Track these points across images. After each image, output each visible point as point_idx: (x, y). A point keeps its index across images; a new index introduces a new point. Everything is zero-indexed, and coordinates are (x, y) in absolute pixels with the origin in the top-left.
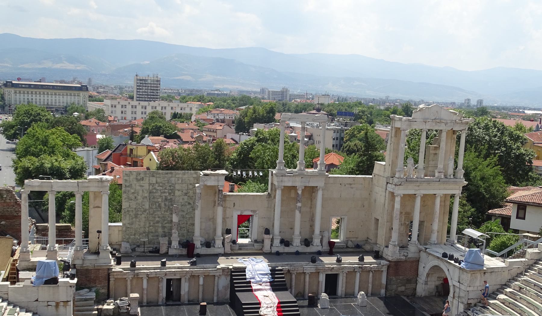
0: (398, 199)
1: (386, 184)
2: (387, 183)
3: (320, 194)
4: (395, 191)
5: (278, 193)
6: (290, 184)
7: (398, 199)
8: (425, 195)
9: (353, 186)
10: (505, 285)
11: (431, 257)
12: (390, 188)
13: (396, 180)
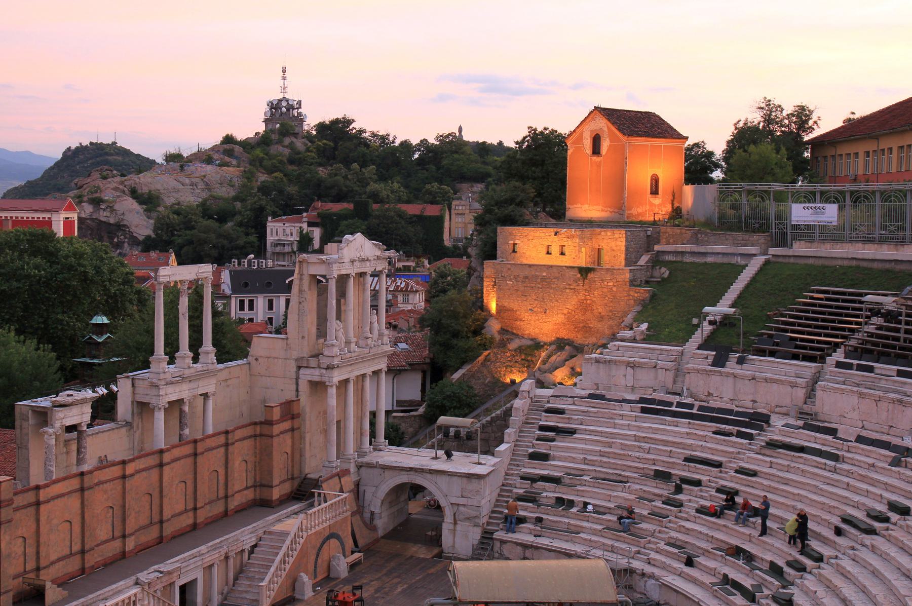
0: (333, 391)
1: (295, 369)
2: (299, 368)
3: (210, 403)
4: (324, 379)
5: (160, 416)
6: (174, 397)
7: (333, 391)
8: (357, 377)
9: (229, 382)
10: (503, 485)
11: (388, 473)
12: (314, 375)
13: (325, 361)
